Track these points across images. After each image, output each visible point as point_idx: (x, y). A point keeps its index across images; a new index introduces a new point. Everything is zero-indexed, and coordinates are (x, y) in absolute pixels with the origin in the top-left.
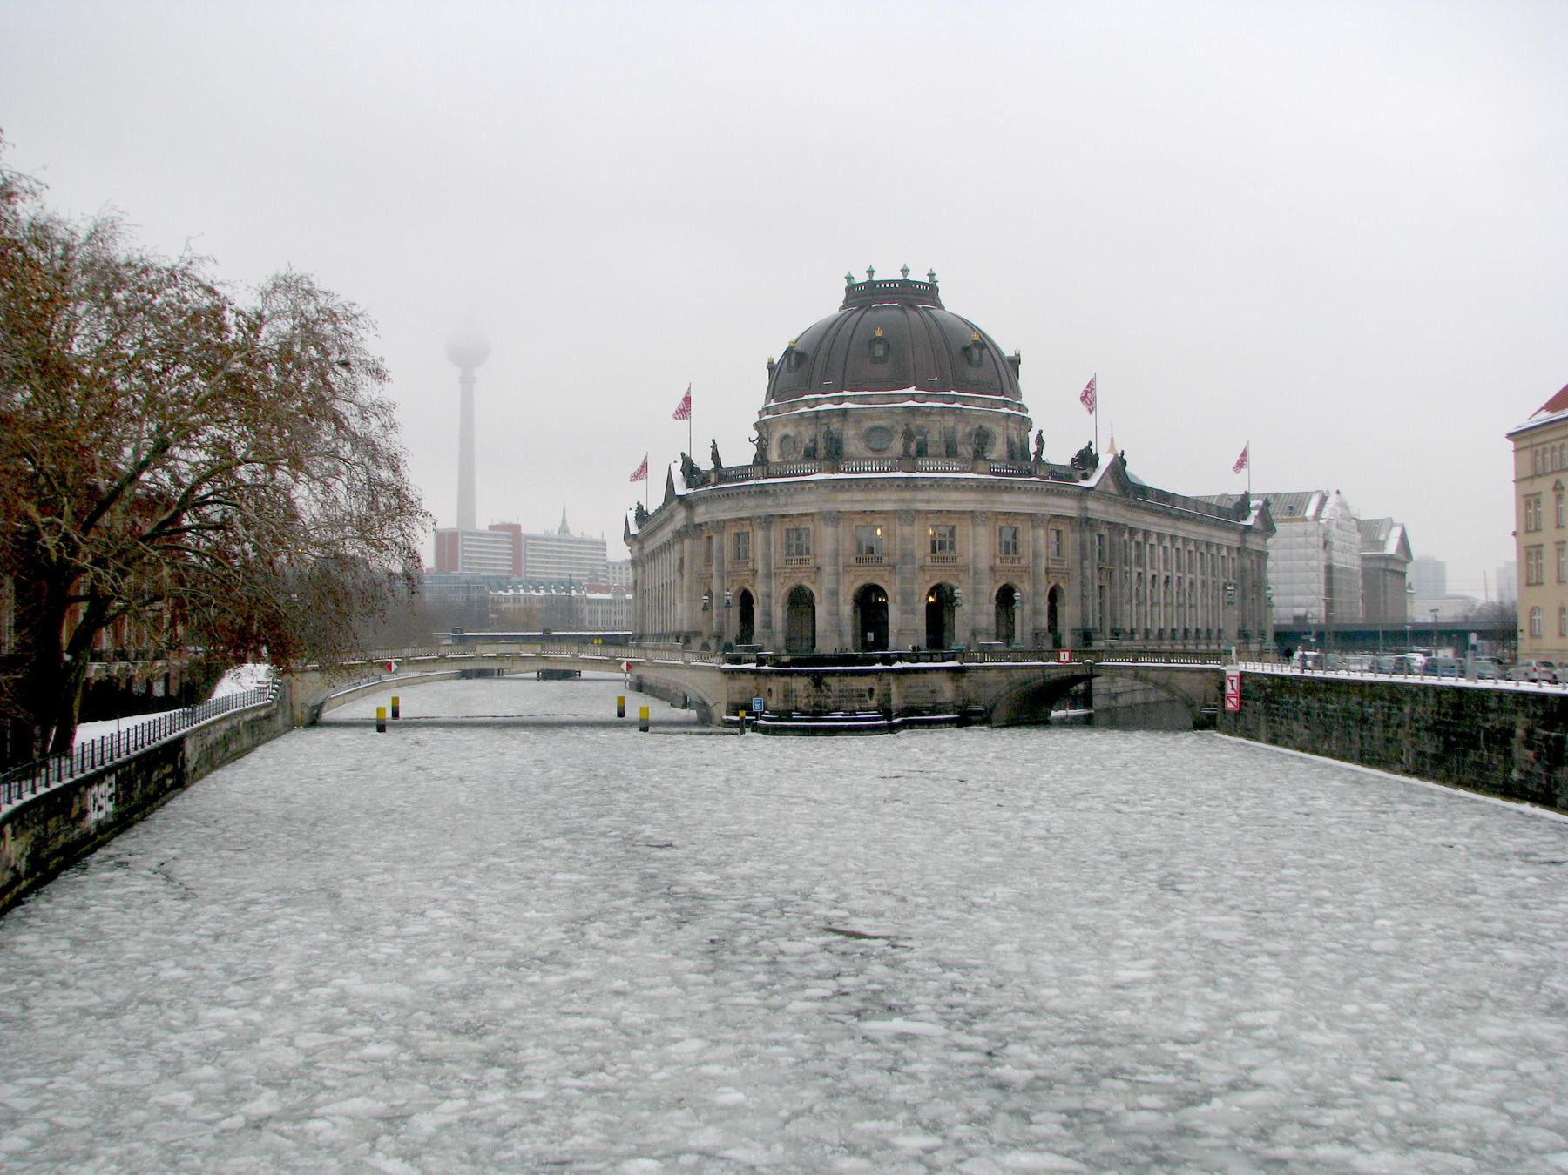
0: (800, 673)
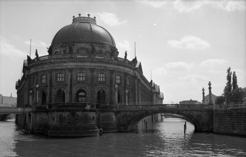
0: (66, 111)
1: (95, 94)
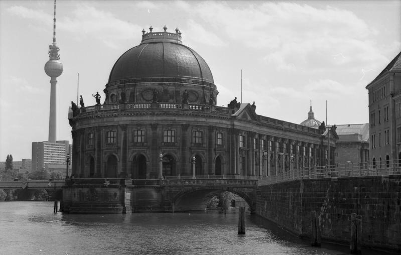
0: (86, 187)
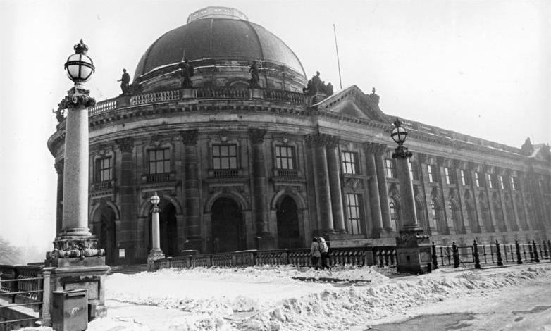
1: (138, 217)
